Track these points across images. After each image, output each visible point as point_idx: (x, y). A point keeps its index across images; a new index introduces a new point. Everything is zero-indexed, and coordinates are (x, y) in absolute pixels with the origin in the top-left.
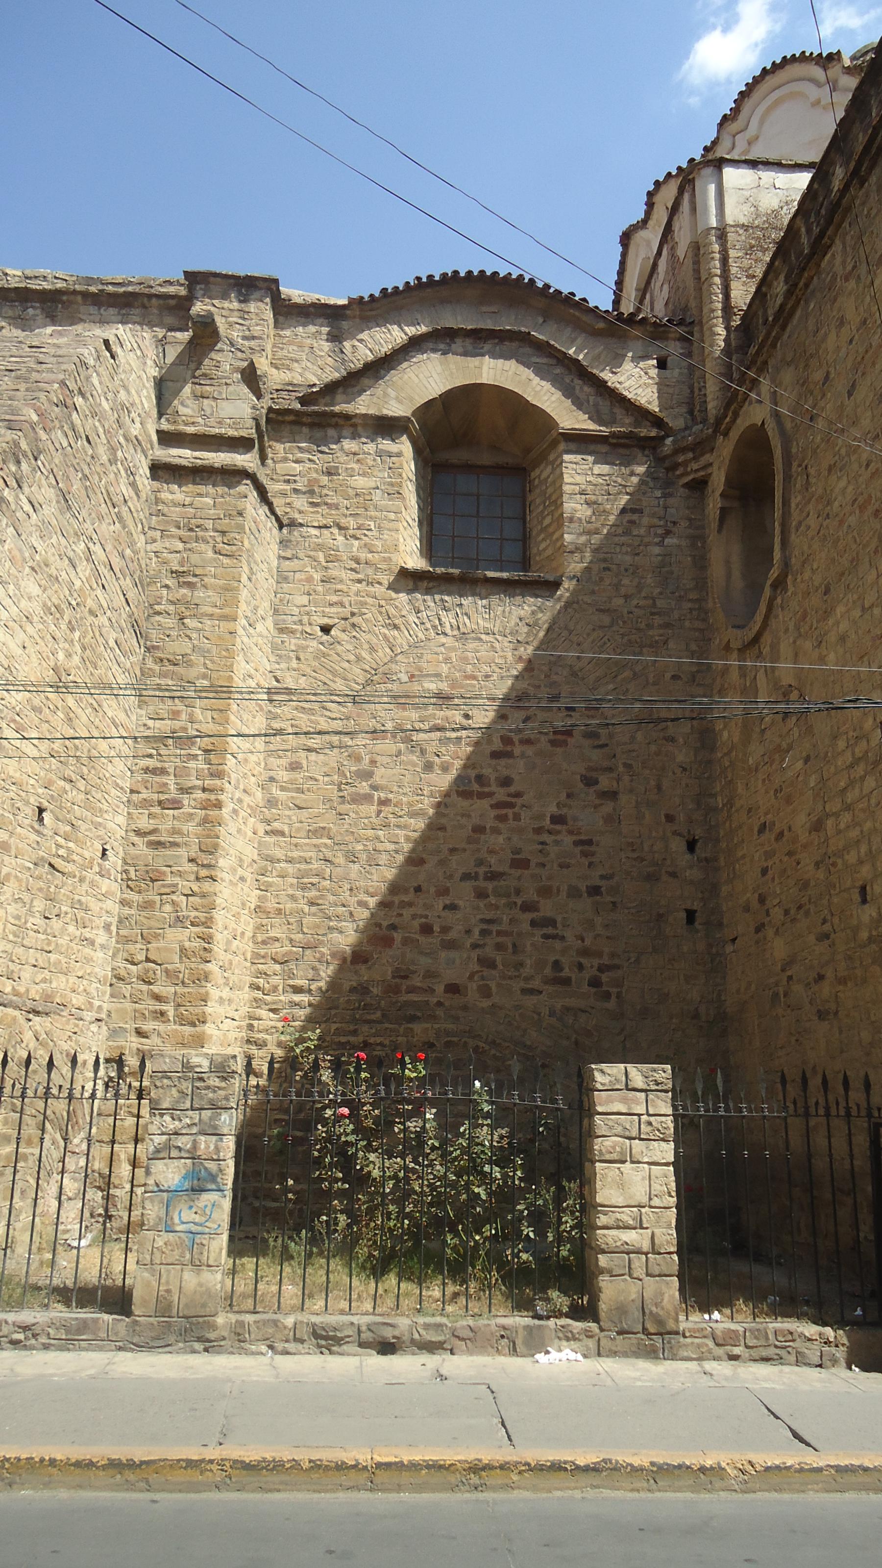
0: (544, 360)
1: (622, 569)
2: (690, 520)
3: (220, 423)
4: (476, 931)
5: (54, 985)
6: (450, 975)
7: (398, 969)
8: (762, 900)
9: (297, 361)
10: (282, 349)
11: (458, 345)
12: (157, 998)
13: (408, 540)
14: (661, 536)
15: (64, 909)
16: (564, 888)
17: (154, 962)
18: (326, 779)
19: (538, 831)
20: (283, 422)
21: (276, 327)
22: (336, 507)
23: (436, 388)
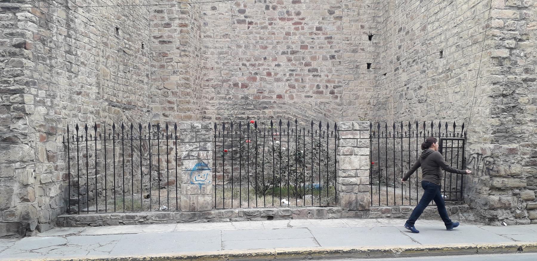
4: (288, 74)
5: (131, 98)
6: (278, 91)
7: (259, 90)
8: (398, 59)
12: (169, 102)
15: (131, 69)
16: (321, 56)
17: (166, 88)
18: (227, 14)
19: (311, 34)
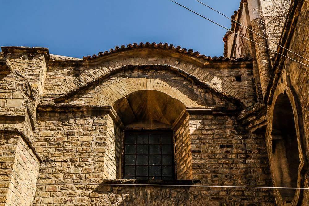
0: (178, 78)
1: (224, 176)
2: (259, 149)
9: (57, 86)
13: (110, 167)
14: (244, 158)
20: (46, 112)
21: (47, 71)
23: (124, 93)
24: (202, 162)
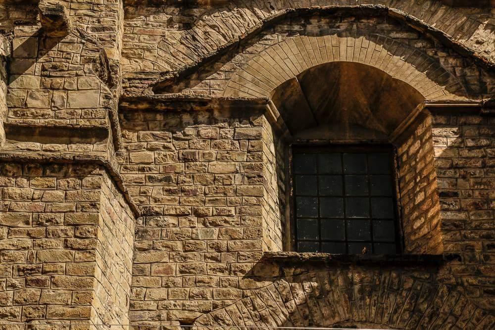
0: (405, 35)
3: (72, 114)
9: (149, 50)
10: (133, 39)
11: (313, 25)
13: (272, 224)
20: (137, 110)
21: (126, 18)
22: (194, 193)
23: (293, 69)
24: (462, 216)
